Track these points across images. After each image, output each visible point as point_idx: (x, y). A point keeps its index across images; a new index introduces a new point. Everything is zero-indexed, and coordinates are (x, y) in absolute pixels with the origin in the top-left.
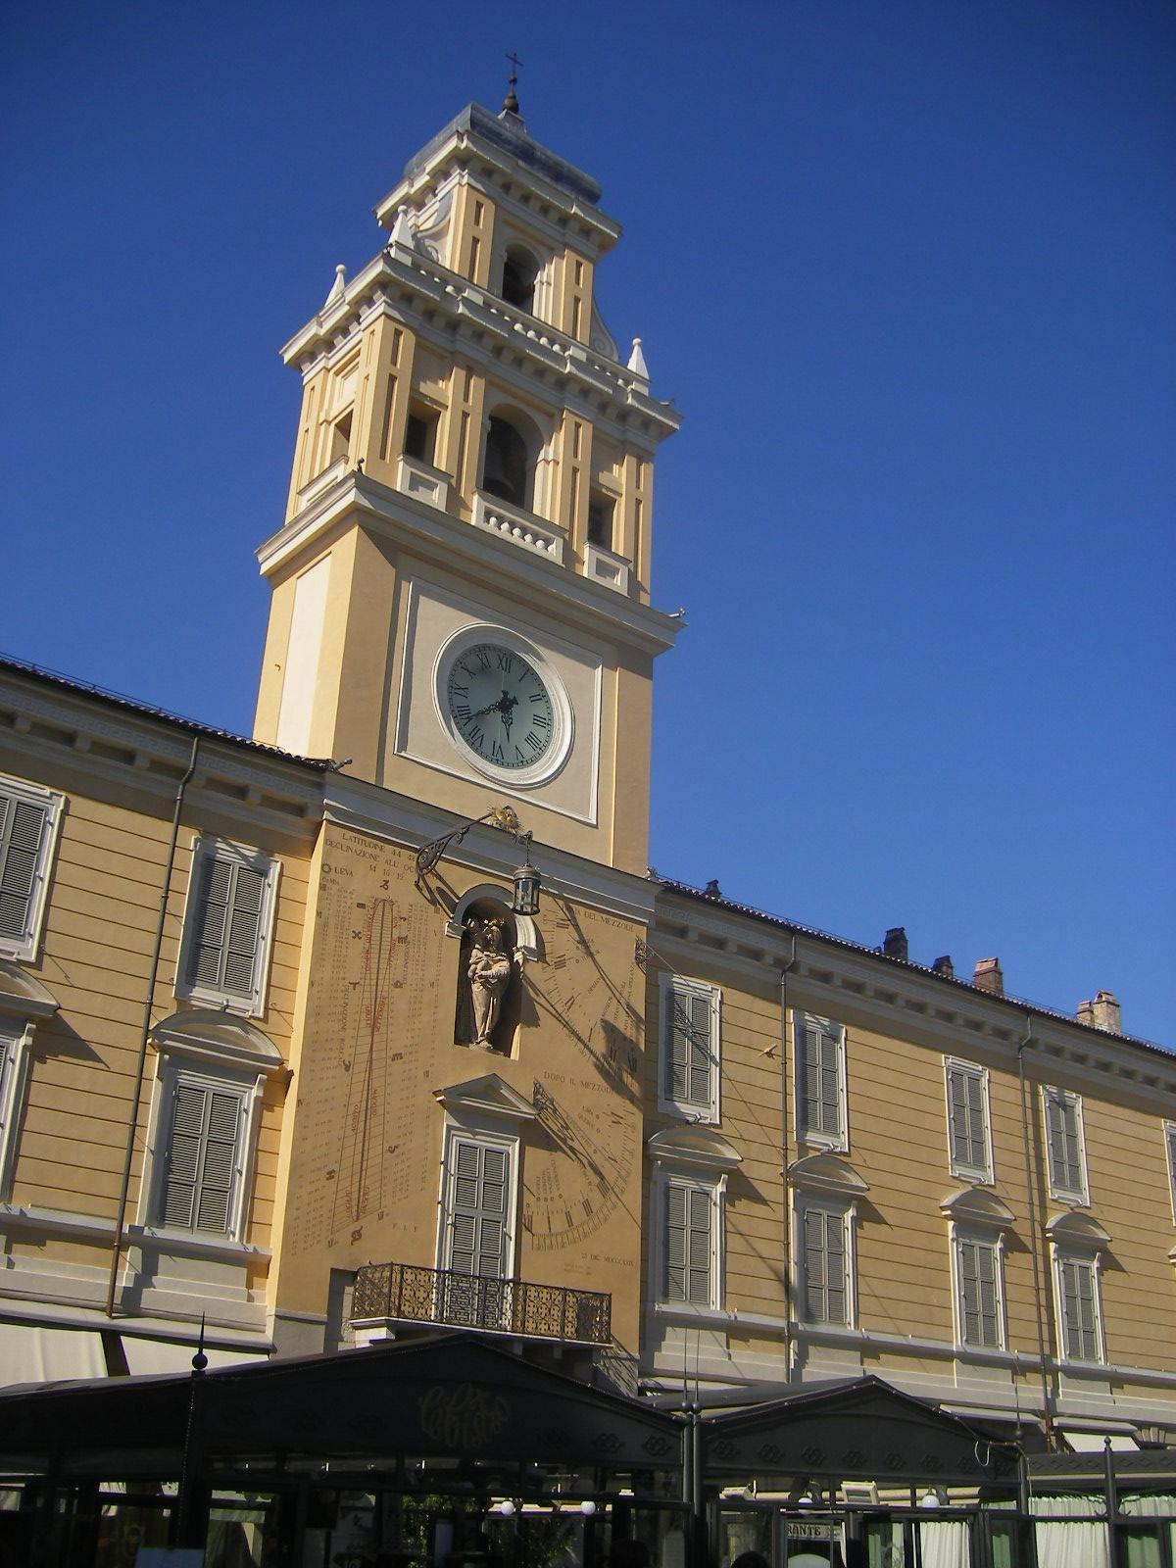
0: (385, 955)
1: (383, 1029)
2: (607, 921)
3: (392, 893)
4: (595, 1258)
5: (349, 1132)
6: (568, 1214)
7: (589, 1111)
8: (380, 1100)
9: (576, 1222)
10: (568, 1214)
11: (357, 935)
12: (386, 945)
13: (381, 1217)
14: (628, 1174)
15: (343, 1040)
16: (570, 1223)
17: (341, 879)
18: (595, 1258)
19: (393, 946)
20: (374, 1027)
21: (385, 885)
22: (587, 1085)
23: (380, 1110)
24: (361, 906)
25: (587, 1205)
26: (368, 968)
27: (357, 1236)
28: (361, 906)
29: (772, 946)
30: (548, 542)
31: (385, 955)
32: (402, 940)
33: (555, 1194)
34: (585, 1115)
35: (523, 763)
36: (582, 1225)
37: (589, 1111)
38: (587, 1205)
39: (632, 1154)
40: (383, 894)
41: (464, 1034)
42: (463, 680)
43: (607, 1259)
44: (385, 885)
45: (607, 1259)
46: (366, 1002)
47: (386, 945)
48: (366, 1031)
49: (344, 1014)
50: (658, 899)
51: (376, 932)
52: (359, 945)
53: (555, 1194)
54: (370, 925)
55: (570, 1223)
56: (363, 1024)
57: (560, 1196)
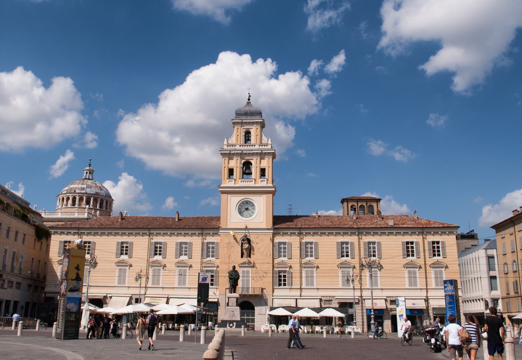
29: (297, 232)
35: (251, 216)
41: (242, 257)
52: (226, 249)
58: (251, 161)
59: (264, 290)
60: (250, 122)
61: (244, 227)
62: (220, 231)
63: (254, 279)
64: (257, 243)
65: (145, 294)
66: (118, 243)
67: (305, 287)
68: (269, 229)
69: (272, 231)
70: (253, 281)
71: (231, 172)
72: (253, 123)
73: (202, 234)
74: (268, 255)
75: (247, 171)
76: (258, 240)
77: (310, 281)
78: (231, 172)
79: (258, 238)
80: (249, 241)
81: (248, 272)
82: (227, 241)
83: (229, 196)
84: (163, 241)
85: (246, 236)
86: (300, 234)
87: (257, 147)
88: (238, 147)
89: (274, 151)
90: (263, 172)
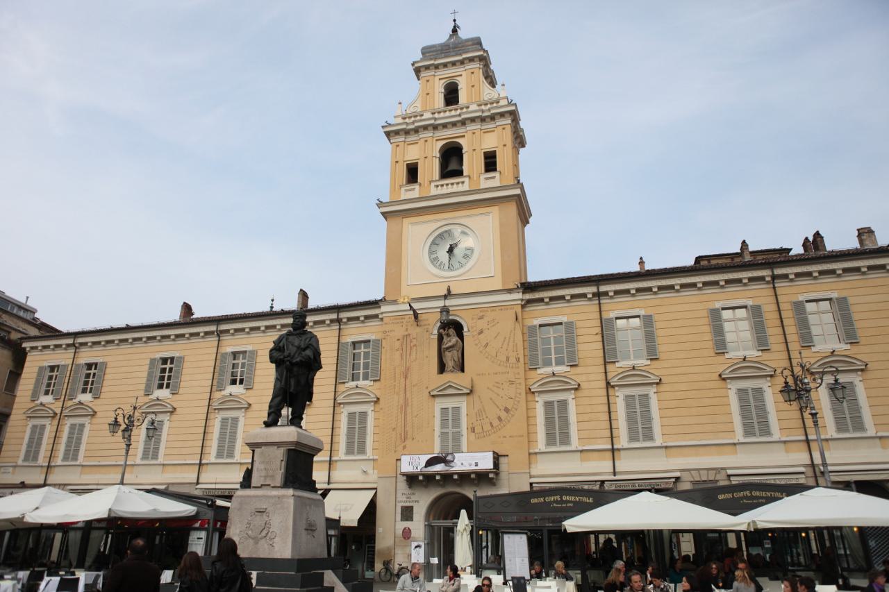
0: (408, 353)
1: (409, 378)
2: (501, 310)
3: (409, 332)
4: (505, 437)
5: (399, 413)
6: (491, 423)
7: (497, 383)
8: (410, 401)
9: (494, 425)
10: (491, 423)
11: (397, 350)
12: (409, 348)
13: (413, 439)
14: (519, 402)
15: (395, 385)
16: (492, 426)
17: (391, 334)
18: (505, 437)
19: (411, 347)
20: (406, 377)
21: (407, 330)
22: (496, 374)
23: (410, 404)
24: (398, 340)
25: (500, 419)
26: (402, 358)
27: (404, 447)
28: (398, 340)
30: (463, 183)
31: (408, 353)
32: (415, 345)
33: (484, 417)
34: (497, 385)
36: (498, 426)
37: (497, 383)
38: (500, 419)
39: (520, 394)
40: (406, 333)
41: (442, 368)
42: (434, 248)
43: (510, 437)
44: (407, 330)
45: (510, 437)
46: (402, 370)
47: (409, 348)
48: (403, 380)
49: (395, 376)
50: (523, 293)
51: (404, 346)
52: (397, 354)
53: (484, 417)
54: (402, 345)
55: (492, 426)
56: (402, 377)
57: (487, 417)
58: (460, 141)
59: (502, 460)
60: (454, 64)
61: (444, 292)
62: (384, 308)
63: (473, 430)
64: (481, 332)
65: (198, 483)
66: (153, 361)
67: (626, 445)
68: (510, 291)
69: (519, 296)
70: (472, 436)
71: (412, 173)
72: (462, 62)
73: (339, 321)
74: (513, 360)
75: (453, 166)
76: (481, 324)
77: (641, 428)
78: (412, 173)
79: (481, 318)
80: (458, 328)
81: (457, 410)
82: (399, 332)
83: (406, 221)
84: (249, 348)
85: (445, 310)
86: (598, 295)
87: (473, 107)
88: (427, 115)
89: (513, 108)
90: (490, 162)
